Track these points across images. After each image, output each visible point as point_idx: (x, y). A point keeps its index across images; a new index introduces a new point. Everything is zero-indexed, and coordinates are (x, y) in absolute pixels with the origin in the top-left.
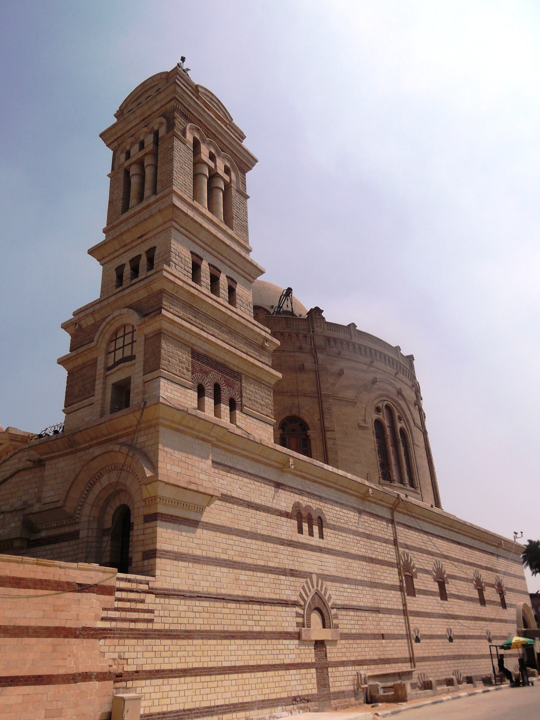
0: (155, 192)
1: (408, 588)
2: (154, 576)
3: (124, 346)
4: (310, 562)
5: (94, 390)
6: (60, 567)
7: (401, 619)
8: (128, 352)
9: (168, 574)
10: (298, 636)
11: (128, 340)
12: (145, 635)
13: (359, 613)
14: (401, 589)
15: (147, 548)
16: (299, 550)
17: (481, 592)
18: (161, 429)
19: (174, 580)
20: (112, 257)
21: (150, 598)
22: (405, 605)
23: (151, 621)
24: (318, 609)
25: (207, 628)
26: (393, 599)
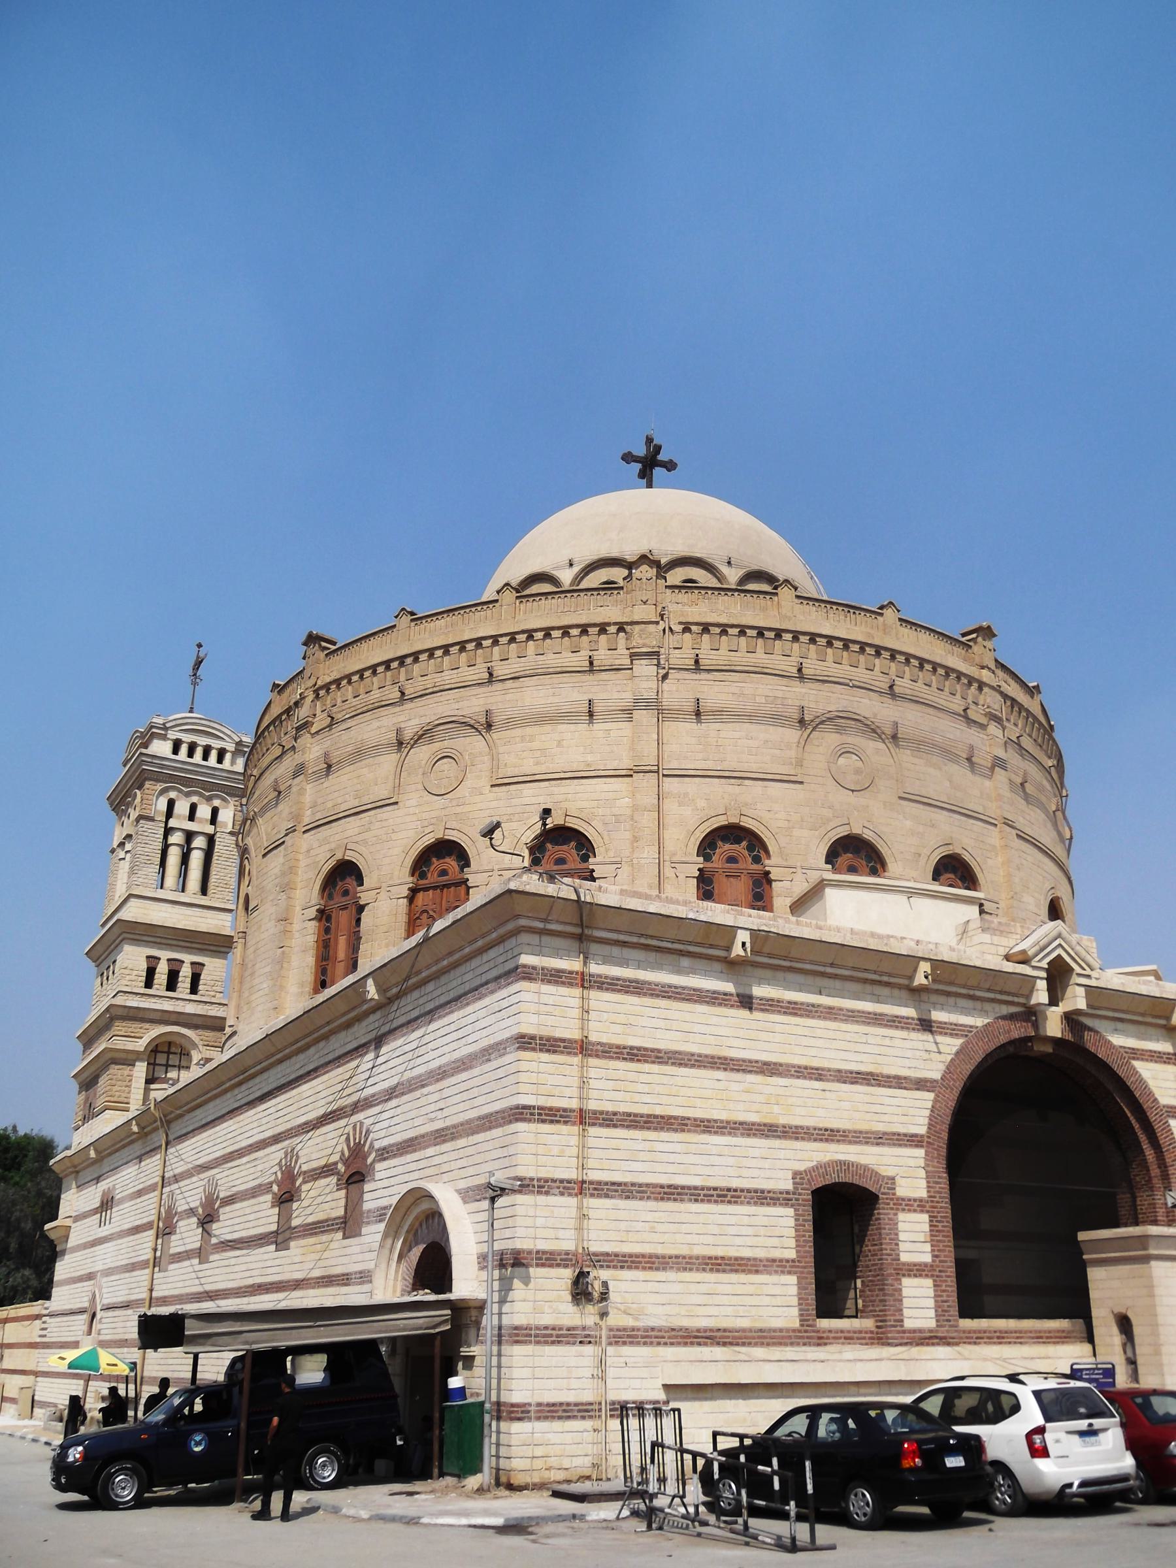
0: (204, 890)
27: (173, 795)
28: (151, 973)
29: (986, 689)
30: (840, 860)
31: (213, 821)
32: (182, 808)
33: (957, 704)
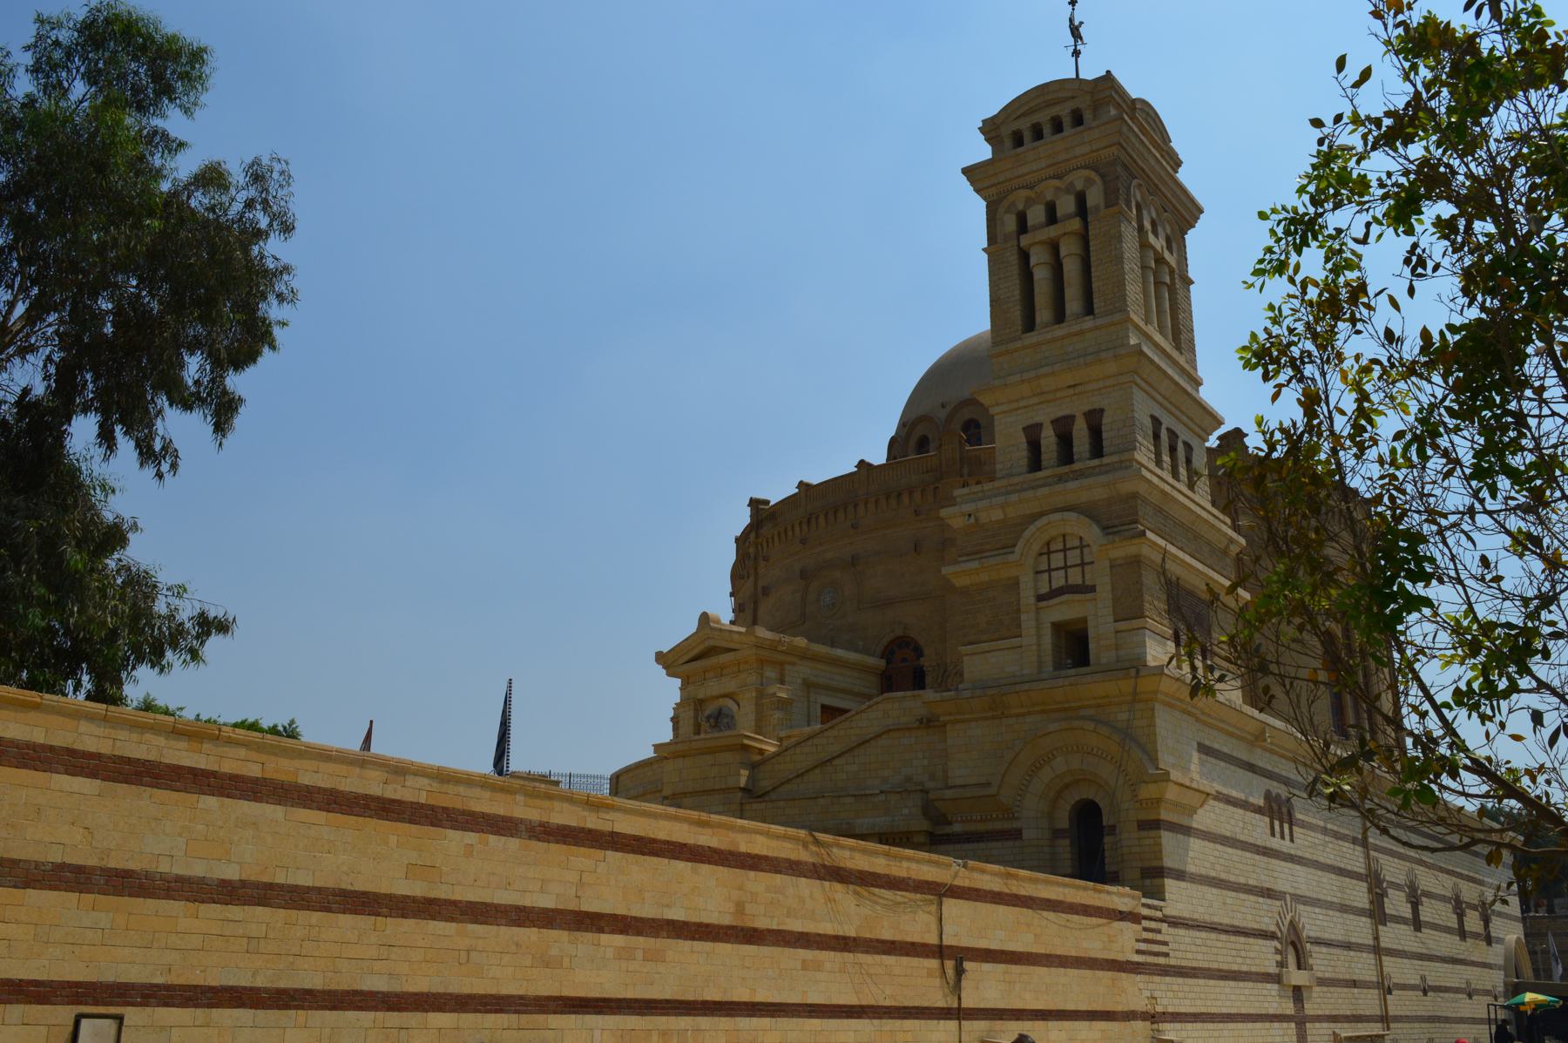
0: (1089, 310)
1: (1378, 914)
2: (1163, 900)
3: (1066, 567)
4: (1285, 877)
5: (1019, 626)
6: (1108, 893)
7: (1368, 959)
8: (1075, 577)
9: (1179, 898)
10: (1277, 979)
11: (1074, 556)
12: (1166, 971)
13: (1332, 950)
14: (1370, 914)
15: (1147, 864)
16: (1274, 861)
17: (1461, 917)
18: (1157, 706)
19: (1180, 906)
20: (1015, 405)
21: (1164, 926)
22: (1377, 938)
23: (1166, 955)
24: (1293, 944)
25: (1206, 965)
26: (1361, 929)
27: (1020, 207)
28: (1035, 447)
31: (1082, 210)
32: (1036, 215)
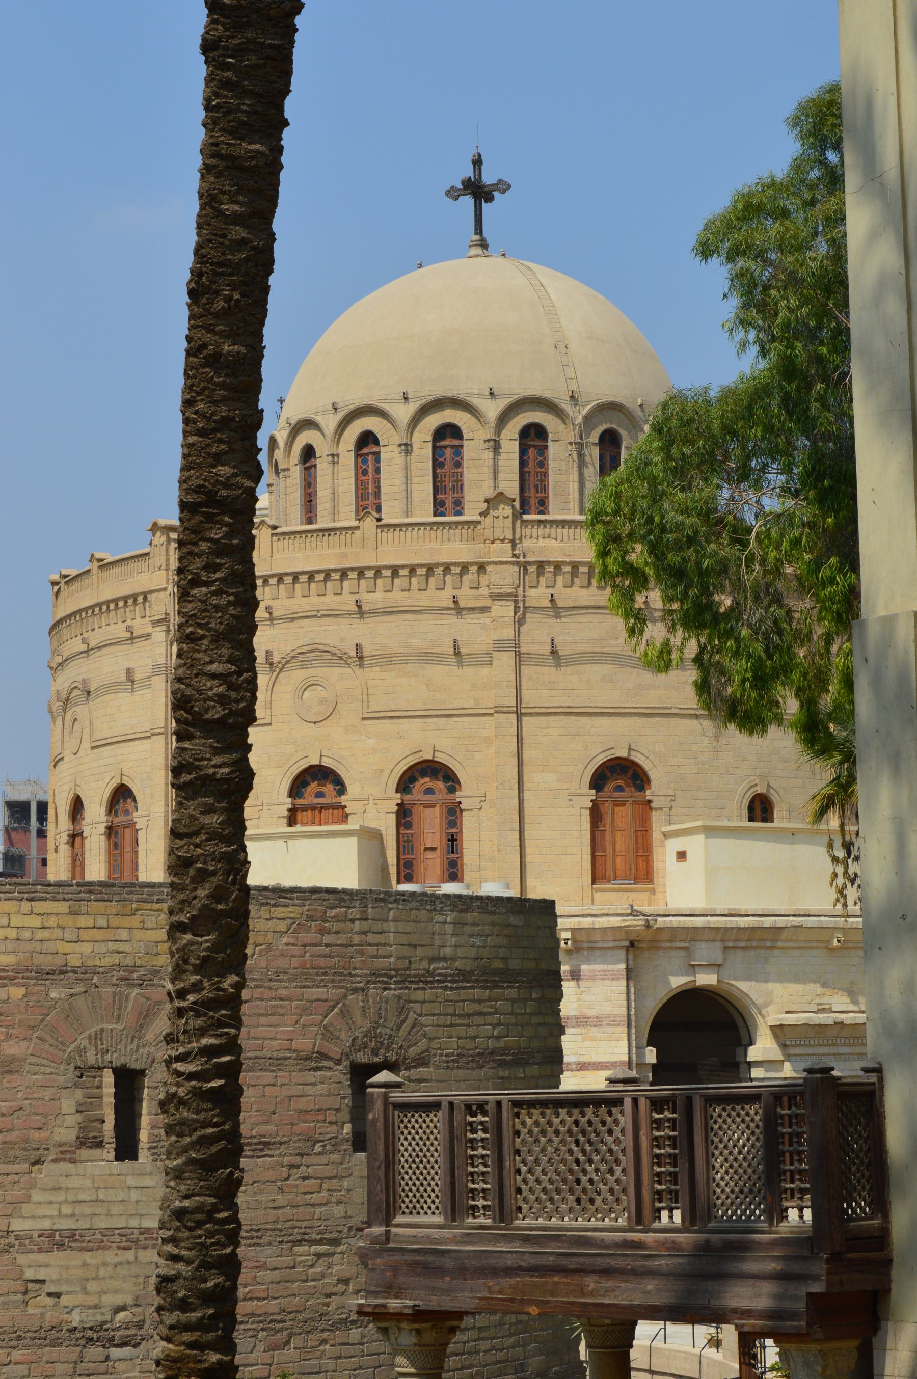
29: (489, 568)
30: (309, 788)
33: (444, 598)
